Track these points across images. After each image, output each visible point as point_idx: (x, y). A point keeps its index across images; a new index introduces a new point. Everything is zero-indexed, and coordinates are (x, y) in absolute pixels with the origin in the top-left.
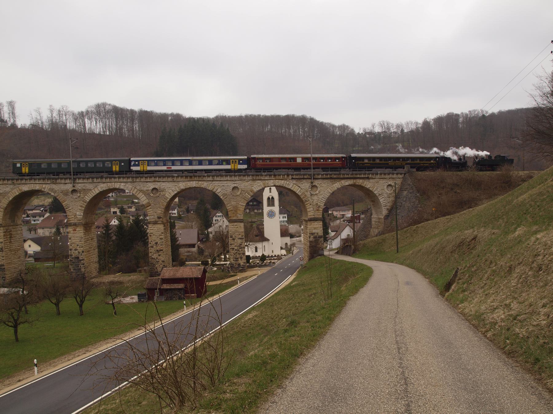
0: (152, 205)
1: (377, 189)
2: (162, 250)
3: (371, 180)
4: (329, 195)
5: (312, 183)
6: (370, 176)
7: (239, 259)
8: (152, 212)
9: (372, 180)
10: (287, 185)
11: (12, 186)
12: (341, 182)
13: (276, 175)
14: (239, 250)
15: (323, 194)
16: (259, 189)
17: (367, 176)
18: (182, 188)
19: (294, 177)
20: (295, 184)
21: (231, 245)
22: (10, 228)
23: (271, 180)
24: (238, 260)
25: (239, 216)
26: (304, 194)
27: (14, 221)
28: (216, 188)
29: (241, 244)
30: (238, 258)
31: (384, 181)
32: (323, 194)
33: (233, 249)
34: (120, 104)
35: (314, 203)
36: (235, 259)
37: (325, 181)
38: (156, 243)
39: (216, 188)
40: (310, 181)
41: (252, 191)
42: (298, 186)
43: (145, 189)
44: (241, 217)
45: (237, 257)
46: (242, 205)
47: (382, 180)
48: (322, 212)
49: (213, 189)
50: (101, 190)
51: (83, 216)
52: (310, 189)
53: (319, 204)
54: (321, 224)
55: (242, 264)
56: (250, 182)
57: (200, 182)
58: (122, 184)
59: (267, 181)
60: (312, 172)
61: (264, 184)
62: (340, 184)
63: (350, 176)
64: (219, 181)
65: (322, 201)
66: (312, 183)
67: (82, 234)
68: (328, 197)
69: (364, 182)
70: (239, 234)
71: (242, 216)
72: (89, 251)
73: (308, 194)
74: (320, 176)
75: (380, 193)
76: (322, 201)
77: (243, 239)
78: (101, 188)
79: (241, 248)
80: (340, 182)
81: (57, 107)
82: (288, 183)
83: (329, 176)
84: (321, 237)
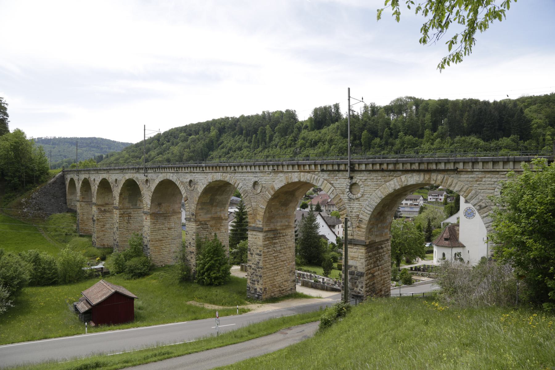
0: (189, 199)
1: (476, 194)
2: (193, 253)
3: (464, 177)
4: (378, 201)
5: (351, 178)
6: (461, 166)
7: (256, 283)
8: (188, 207)
9: (466, 176)
10: (315, 181)
11: (122, 175)
12: (401, 178)
13: (300, 165)
14: (256, 270)
15: (369, 200)
16: (281, 186)
17: (451, 166)
18: (209, 181)
19: (325, 167)
20: (326, 180)
21: (249, 260)
22: (129, 210)
23: (296, 173)
24: (255, 284)
25: (258, 223)
26: (339, 196)
27: (136, 205)
28: (238, 182)
29: (259, 263)
30: (255, 281)
31: (494, 178)
32: (369, 200)
33: (251, 266)
34: (418, 96)
35: (354, 214)
36: (252, 282)
37: (374, 175)
38: (190, 243)
39: (238, 182)
40: (347, 174)
41: (273, 188)
42: (330, 183)
43: (185, 180)
44: (260, 224)
45: (254, 279)
46: (261, 208)
47: (489, 176)
48: (364, 230)
49: (235, 184)
50: (160, 181)
51: (151, 206)
52: (348, 190)
53: (361, 216)
54: (362, 253)
55: (258, 290)
56: (271, 175)
57: (224, 174)
58: (172, 175)
59: (290, 174)
60: (348, 160)
61: (286, 178)
62: (397, 181)
63: (415, 167)
64: (241, 173)
65: (366, 211)
66: (351, 178)
67: (149, 223)
68: (376, 204)
69: (447, 180)
70: (258, 248)
71: (261, 223)
72: (162, 240)
73: (345, 197)
74: (363, 167)
75: (484, 205)
76: (366, 211)
77: (260, 255)
78: (160, 178)
79: (258, 268)
80: (399, 178)
81: (368, 104)
82: (316, 177)
83: (377, 167)
84: (361, 275)
